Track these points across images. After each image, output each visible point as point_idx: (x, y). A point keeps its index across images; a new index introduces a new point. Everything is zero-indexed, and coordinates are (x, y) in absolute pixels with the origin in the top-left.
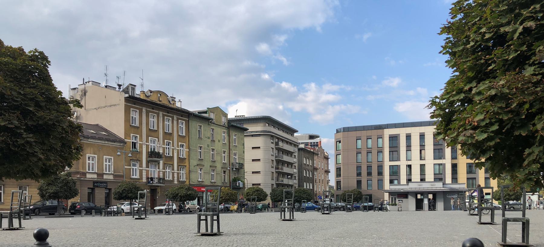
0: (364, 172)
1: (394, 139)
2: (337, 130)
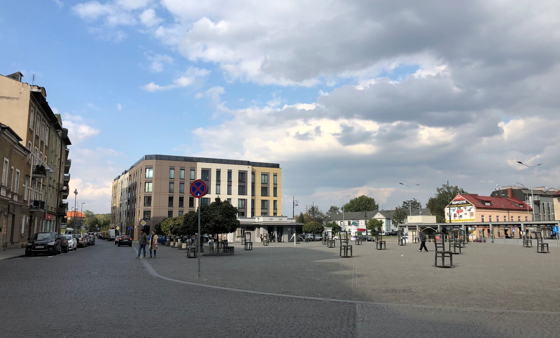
0: (176, 201)
1: (206, 172)
2: (146, 156)
